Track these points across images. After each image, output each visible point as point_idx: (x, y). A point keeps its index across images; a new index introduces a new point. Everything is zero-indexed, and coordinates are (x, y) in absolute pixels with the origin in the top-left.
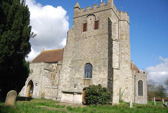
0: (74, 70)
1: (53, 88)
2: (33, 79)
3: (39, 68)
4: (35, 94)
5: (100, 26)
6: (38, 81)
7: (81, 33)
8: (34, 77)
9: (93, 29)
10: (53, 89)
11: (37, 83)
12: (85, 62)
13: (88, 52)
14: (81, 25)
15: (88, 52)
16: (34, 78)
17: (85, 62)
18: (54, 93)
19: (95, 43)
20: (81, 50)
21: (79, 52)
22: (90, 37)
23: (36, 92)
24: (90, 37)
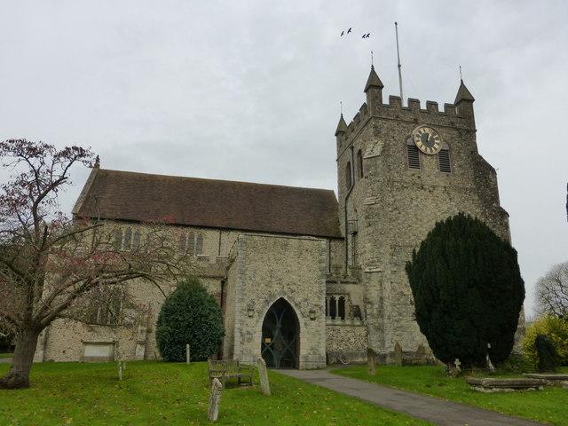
4: (312, 349)
5: (455, 165)
8: (293, 287)
10: (348, 329)
18: (352, 340)
22: (434, 187)
24: (434, 187)
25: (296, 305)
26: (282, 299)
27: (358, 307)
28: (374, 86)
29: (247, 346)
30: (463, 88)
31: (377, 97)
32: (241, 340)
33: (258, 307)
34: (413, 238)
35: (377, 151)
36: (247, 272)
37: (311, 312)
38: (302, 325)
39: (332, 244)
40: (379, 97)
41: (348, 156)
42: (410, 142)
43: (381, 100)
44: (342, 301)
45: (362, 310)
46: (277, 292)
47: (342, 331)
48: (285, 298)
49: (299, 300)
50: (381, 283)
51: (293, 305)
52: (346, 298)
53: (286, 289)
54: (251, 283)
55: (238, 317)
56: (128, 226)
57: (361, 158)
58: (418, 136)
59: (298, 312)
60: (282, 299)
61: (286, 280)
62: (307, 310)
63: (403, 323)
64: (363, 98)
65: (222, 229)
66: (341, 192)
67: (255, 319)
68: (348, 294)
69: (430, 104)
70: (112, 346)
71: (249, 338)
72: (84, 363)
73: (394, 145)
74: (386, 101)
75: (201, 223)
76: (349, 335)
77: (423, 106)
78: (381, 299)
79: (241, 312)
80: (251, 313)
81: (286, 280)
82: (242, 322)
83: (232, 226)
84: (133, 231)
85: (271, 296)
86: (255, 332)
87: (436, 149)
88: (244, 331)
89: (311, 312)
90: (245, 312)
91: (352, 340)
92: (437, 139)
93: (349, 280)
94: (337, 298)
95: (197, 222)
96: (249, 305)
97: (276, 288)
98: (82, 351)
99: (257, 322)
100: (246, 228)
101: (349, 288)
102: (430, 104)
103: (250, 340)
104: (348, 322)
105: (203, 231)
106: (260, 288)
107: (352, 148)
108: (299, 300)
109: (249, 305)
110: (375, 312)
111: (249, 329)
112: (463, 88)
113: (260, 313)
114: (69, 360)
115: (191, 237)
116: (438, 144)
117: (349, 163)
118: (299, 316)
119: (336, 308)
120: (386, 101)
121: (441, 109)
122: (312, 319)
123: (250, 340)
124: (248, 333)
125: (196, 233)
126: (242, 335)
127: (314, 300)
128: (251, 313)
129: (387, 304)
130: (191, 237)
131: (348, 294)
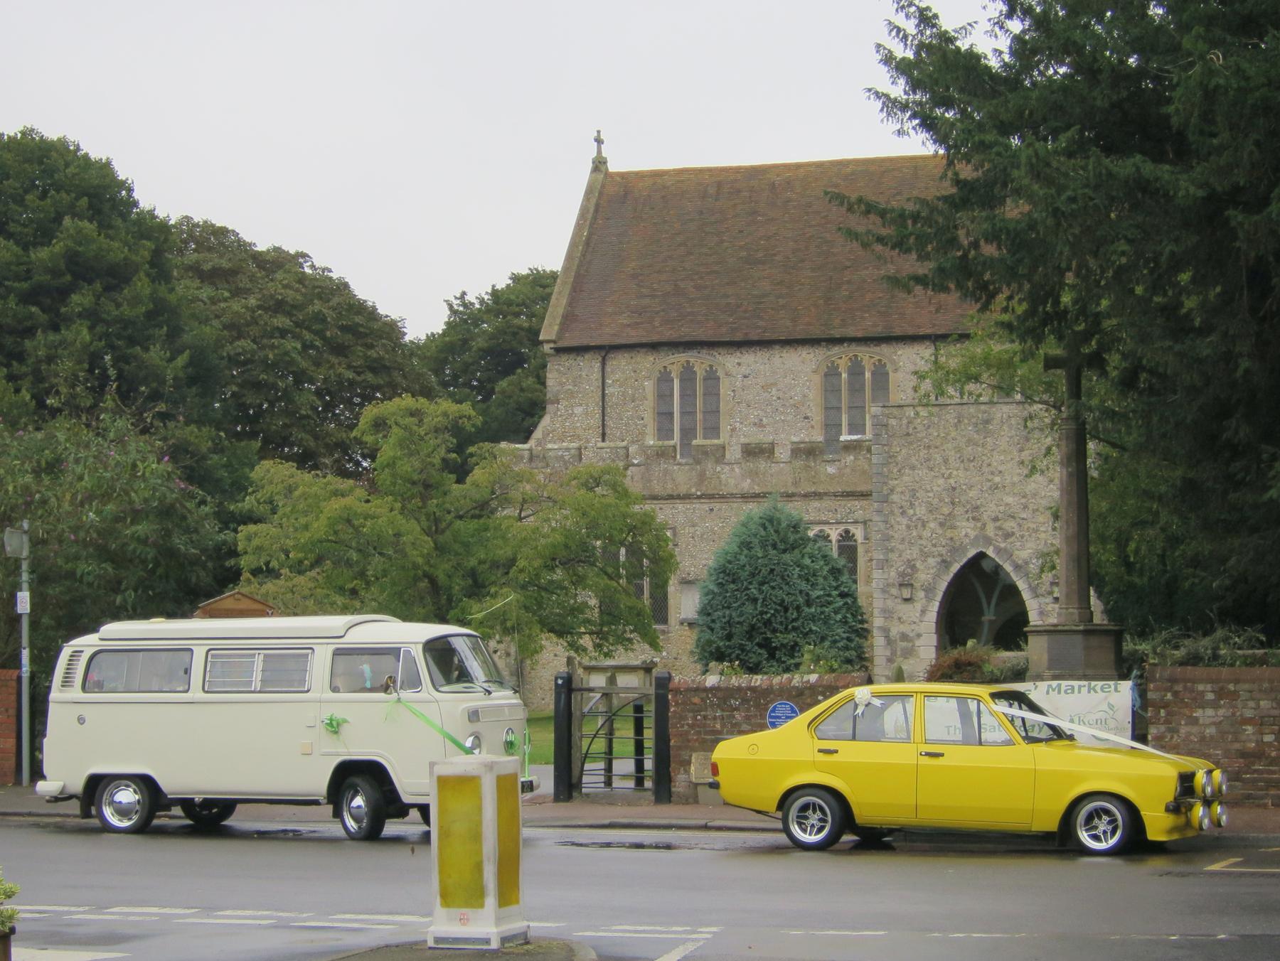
2: (999, 551)
8: (1010, 525)
25: (1017, 567)
26: (982, 555)
32: (888, 653)
33: (923, 577)
36: (895, 497)
46: (968, 539)
53: (990, 531)
54: (905, 521)
55: (878, 604)
56: (681, 358)
60: (982, 555)
61: (991, 509)
67: (918, 606)
70: (641, 674)
75: (879, 330)
79: (884, 591)
80: (906, 593)
81: (991, 509)
82: (888, 614)
84: (700, 372)
85: (955, 550)
86: (919, 636)
88: (895, 631)
90: (894, 591)
95: (869, 324)
96: (902, 575)
97: (966, 529)
99: (923, 612)
105: (885, 349)
106: (926, 534)
108: (1023, 554)
109: (902, 575)
111: (903, 628)
113: (929, 590)
115: (856, 370)
123: (909, 653)
124: (904, 637)
125: (868, 356)
126: (889, 641)
128: (906, 593)
130: (856, 370)
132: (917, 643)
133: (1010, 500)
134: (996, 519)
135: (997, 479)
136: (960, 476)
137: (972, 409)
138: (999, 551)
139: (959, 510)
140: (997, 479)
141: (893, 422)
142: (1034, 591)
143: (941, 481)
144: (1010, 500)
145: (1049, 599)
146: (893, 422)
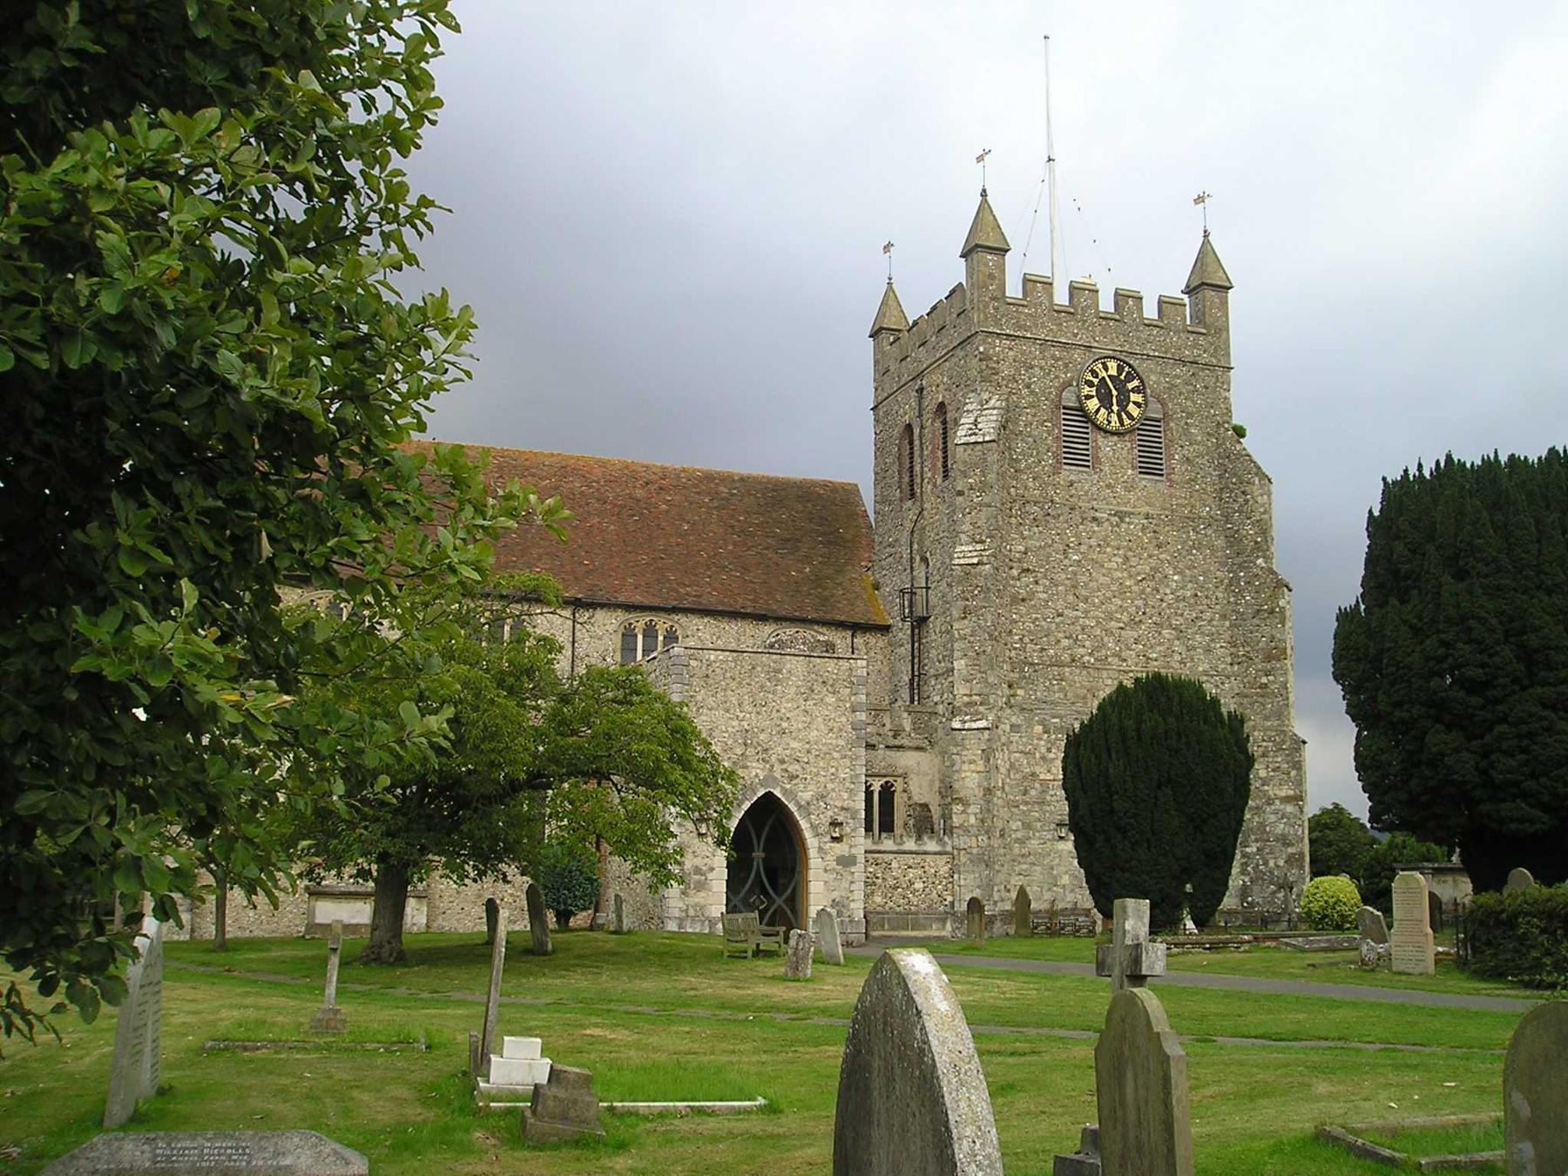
0: (1039, 729)
1: (911, 853)
3: (831, 699)
4: (834, 903)
5: (1175, 460)
6: (839, 804)
7: (1056, 471)
9: (1133, 468)
10: (910, 859)
11: (840, 819)
12: (1109, 682)
13: (1119, 620)
14: (1045, 405)
15: (1119, 620)
16: (792, 777)
17: (1109, 682)
18: (919, 885)
19: (1155, 569)
20: (1071, 598)
21: (1060, 605)
23: (836, 895)
24: (1121, 516)
25: (800, 807)
26: (769, 795)
27: (925, 806)
28: (984, 246)
29: (698, 898)
30: (1206, 256)
31: (991, 276)
34: (1065, 642)
35: (988, 427)
37: (834, 824)
38: (812, 853)
39: (859, 640)
40: (998, 276)
41: (906, 410)
42: (1069, 399)
43: (1002, 287)
44: (887, 793)
45: (936, 812)
47: (894, 865)
48: (777, 793)
49: (807, 796)
50: (987, 755)
51: (792, 807)
52: (898, 786)
57: (944, 422)
58: (1090, 384)
59: (804, 824)
60: (769, 795)
62: (825, 819)
63: (1034, 844)
64: (957, 273)
65: (577, 604)
66: (881, 500)
68: (904, 776)
69: (1121, 297)
71: (699, 881)
72: (178, 942)
73: (1031, 406)
74: (1014, 289)
76: (911, 874)
77: (1106, 304)
78: (989, 791)
83: (602, 596)
86: (712, 869)
87: (1130, 417)
89: (834, 824)
91: (919, 885)
92: (1136, 390)
93: (906, 742)
94: (877, 786)
98: (310, 913)
100: (638, 599)
101: (907, 760)
102: (1121, 297)
103: (702, 886)
104: (910, 845)
107: (921, 390)
108: (806, 796)
110: (972, 820)
111: (698, 861)
112: (1206, 256)
114: (247, 934)
116: (1138, 404)
117: (909, 427)
118: (807, 834)
119: (882, 812)
120: (1014, 289)
121: (1150, 311)
122: (834, 839)
123: (702, 886)
124: (698, 871)
127: (839, 798)
129: (1000, 802)
131: (904, 776)
132: (710, 876)
133: (794, 744)
134: (782, 762)
135: (785, 725)
136: (750, 719)
137: (765, 658)
138: (785, 791)
139: (750, 751)
140: (785, 725)
141: (693, 663)
142: (813, 827)
143: (735, 723)
144: (794, 744)
145: (828, 838)
146: (693, 663)
